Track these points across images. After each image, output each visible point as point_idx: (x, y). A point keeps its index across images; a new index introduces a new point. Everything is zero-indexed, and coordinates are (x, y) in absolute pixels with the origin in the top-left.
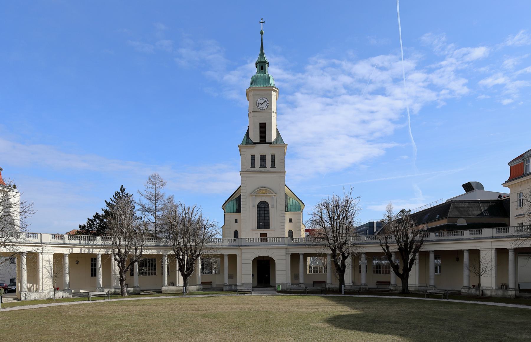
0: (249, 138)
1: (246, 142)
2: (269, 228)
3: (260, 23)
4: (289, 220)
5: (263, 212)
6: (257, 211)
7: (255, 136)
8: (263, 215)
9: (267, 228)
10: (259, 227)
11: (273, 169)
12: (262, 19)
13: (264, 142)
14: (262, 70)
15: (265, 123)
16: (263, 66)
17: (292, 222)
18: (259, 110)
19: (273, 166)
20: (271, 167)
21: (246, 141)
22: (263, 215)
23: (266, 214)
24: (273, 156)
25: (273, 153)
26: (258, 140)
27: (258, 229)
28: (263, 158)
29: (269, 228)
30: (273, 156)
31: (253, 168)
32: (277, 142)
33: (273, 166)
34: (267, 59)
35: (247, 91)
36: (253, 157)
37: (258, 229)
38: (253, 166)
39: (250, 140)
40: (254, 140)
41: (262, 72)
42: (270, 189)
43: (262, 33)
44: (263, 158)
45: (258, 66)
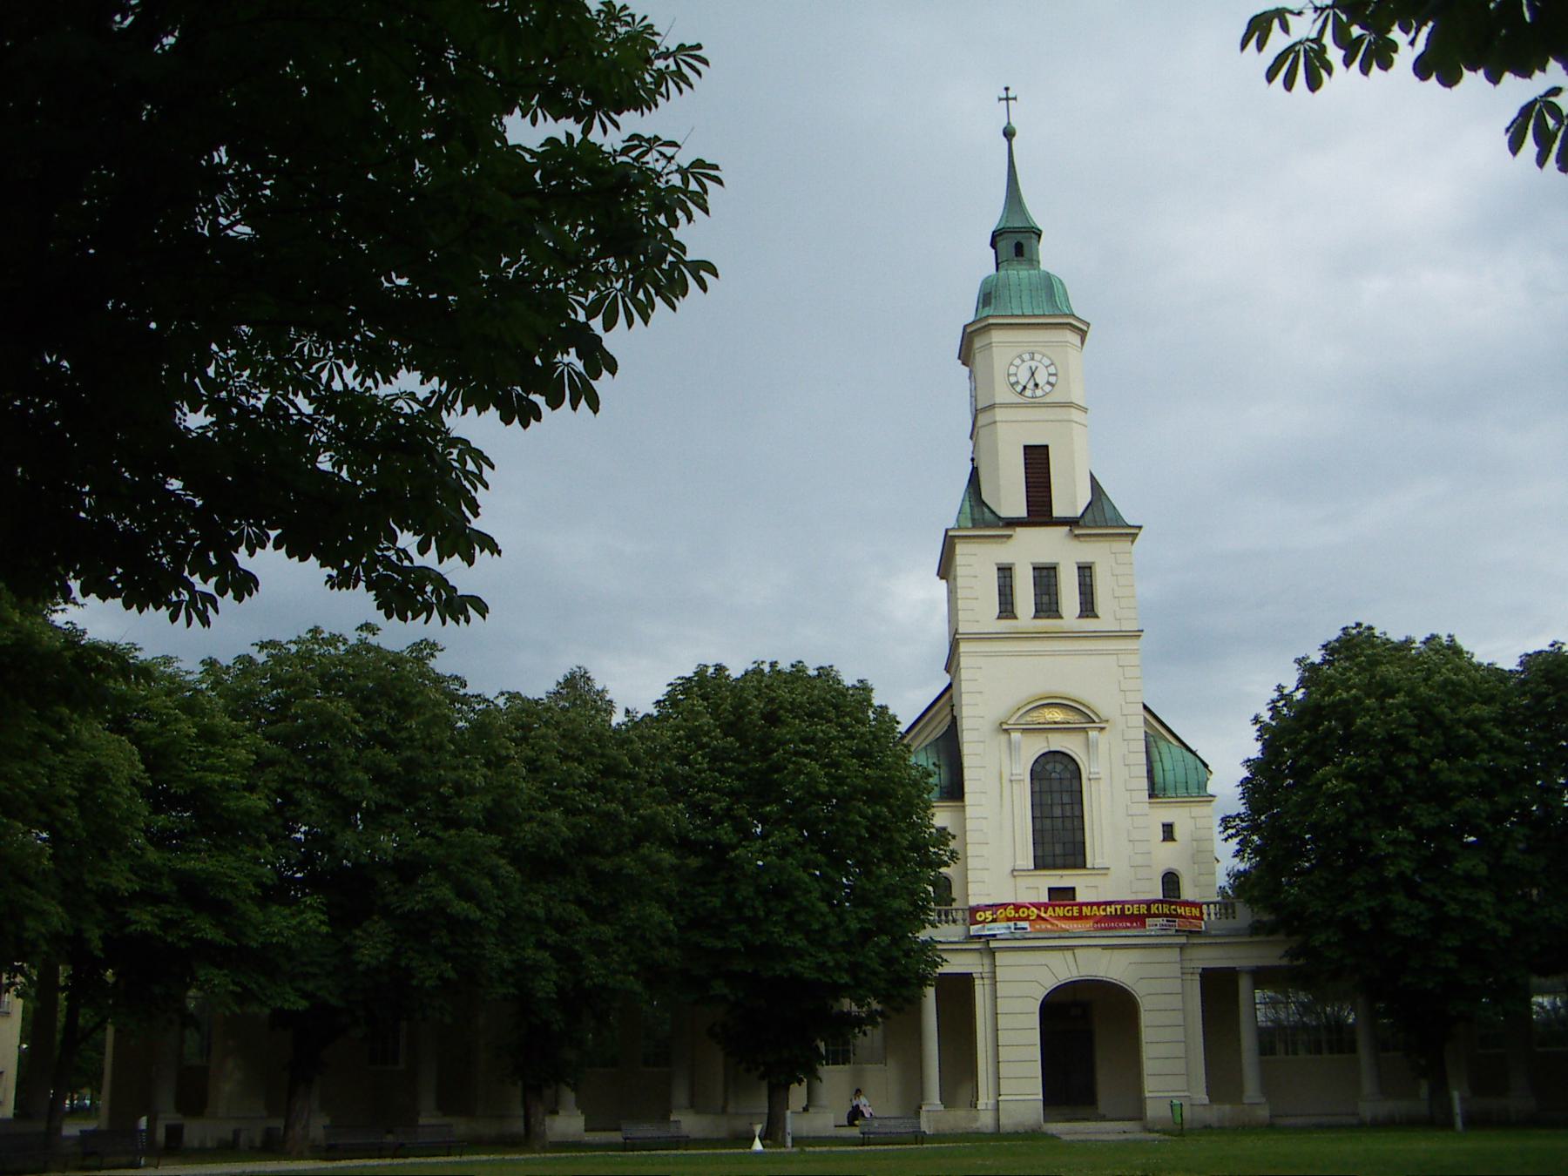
0: (984, 502)
1: (973, 520)
2: (1084, 866)
3: (1000, 99)
4: (1164, 832)
5: (1056, 796)
6: (1032, 792)
7: (1011, 498)
8: (1057, 812)
9: (1075, 867)
10: (1041, 863)
11: (1089, 624)
12: (1007, 89)
13: (1046, 519)
14: (1020, 258)
15: (1047, 447)
16: (1023, 241)
17: (1174, 840)
18: (1021, 400)
19: (1088, 608)
20: (1080, 616)
21: (972, 514)
22: (1057, 812)
23: (1068, 807)
24: (1085, 571)
25: (1086, 558)
26: (1021, 511)
27: (1036, 867)
28: (1046, 576)
29: (1084, 866)
30: (1085, 571)
31: (1006, 618)
32: (1098, 519)
33: (1088, 608)
34: (1038, 214)
35: (968, 330)
36: (1005, 572)
37: (1036, 867)
38: (1007, 609)
39: (986, 510)
40: (1005, 512)
41: (1020, 263)
42: (1084, 705)
43: (1009, 134)
44: (1046, 576)
45: (1001, 245)
